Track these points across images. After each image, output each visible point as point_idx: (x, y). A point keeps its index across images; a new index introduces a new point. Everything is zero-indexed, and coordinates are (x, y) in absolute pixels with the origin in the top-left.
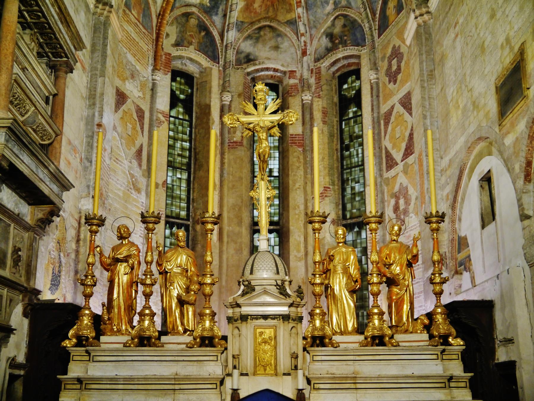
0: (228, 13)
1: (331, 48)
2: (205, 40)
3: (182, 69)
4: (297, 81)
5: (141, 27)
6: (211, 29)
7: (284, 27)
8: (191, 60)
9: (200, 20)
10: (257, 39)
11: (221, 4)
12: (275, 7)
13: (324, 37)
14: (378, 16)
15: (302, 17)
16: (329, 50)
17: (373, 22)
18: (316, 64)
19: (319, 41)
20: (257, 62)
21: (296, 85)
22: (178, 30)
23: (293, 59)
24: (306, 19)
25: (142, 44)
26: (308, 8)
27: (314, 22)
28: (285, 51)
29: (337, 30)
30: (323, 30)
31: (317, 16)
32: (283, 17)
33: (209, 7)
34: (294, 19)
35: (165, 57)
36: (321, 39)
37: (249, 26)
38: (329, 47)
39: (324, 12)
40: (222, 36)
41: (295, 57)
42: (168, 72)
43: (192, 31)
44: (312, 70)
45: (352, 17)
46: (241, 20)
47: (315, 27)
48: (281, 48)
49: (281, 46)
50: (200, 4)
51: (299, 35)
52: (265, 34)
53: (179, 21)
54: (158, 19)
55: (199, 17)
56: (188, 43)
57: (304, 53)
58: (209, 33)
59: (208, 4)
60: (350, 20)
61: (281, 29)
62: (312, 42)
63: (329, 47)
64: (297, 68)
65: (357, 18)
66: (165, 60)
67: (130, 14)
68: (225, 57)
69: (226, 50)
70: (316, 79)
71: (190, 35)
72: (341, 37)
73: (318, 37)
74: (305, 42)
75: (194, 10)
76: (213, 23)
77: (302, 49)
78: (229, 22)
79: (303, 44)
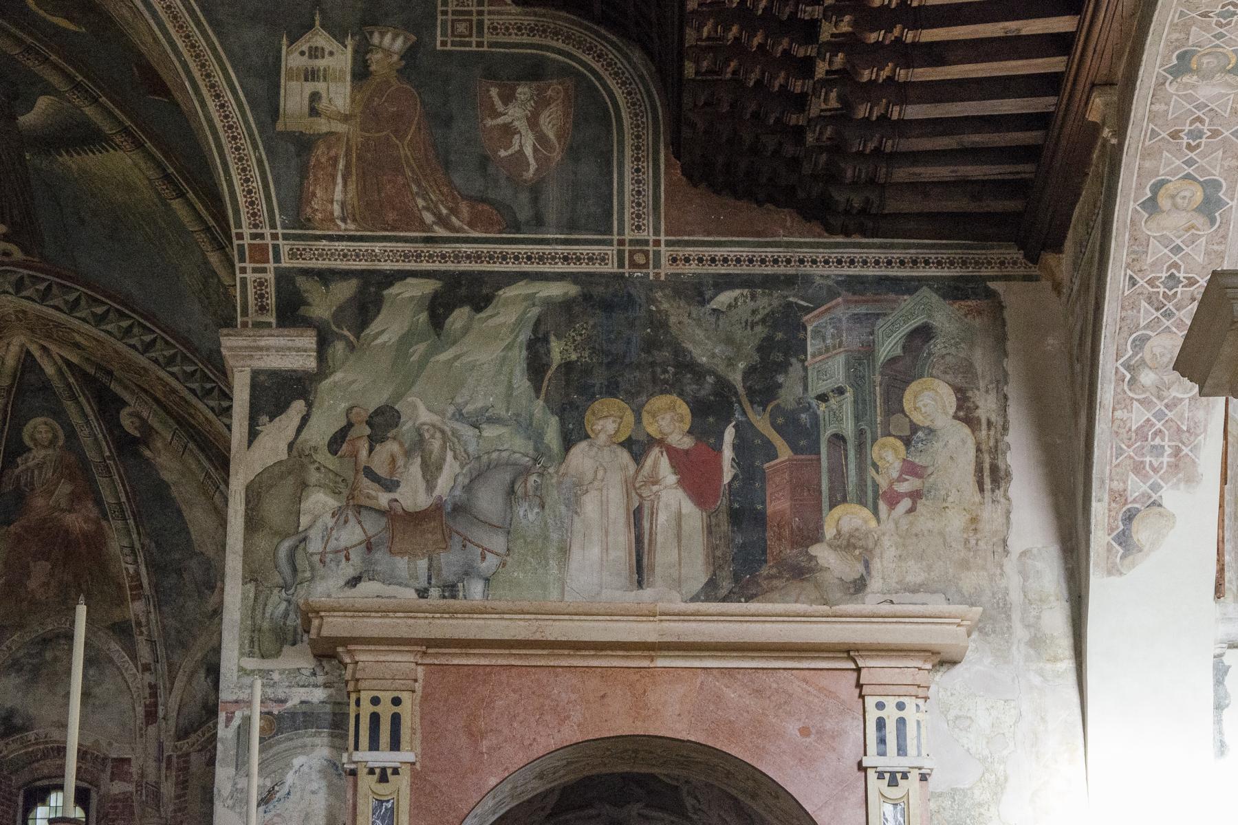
4: (131, 788)
10: (36, 672)
15: (144, 623)
19: (189, 681)
20: (31, 735)
21: (126, 799)
26: (161, 598)
27: (179, 632)
37: (15, 637)
47: (184, 645)
48: (95, 697)
57: (151, 715)
62: (173, 684)
70: (177, 784)
74: (153, 688)
77: (146, 706)
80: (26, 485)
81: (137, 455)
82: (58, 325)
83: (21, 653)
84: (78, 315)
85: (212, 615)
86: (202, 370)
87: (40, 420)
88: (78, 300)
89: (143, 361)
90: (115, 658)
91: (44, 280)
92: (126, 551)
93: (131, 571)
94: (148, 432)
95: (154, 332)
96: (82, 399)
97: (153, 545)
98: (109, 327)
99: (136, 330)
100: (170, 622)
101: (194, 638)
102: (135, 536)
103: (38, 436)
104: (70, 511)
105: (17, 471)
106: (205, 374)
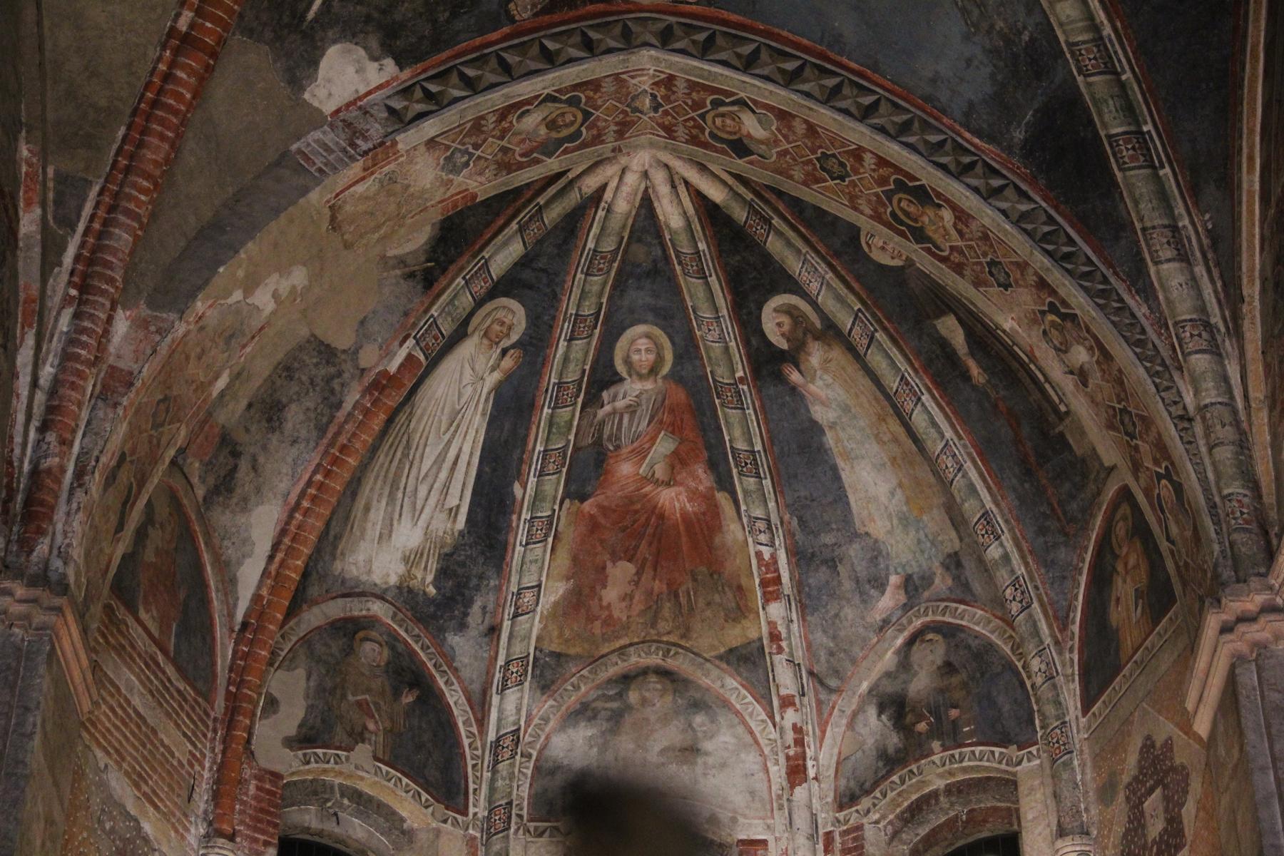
0: (507, 624)
1: (898, 751)
2: (415, 722)
3: (320, 833)
5: (170, 670)
6: (441, 682)
7: (715, 672)
8: (358, 797)
9: (400, 648)
10: (616, 718)
11: (477, 588)
12: (683, 600)
13: (872, 711)
14: (1076, 628)
15: (784, 635)
16: (891, 761)
17: (1060, 653)
18: (841, 815)
19: (851, 725)
22: (312, 684)
23: (752, 793)
24: (795, 641)
25: (170, 735)
26: (806, 603)
27: (831, 654)
28: (723, 765)
29: (921, 684)
30: (865, 686)
31: (842, 633)
32: (710, 639)
33: (432, 601)
34: (758, 644)
35: (258, 788)
36: (860, 717)
37: (584, 672)
38: (891, 750)
39: (868, 620)
40: (480, 706)
41: (761, 786)
42: (266, 844)
43: (368, 690)
44: (829, 837)
45: (977, 636)
46: (555, 647)
48: (707, 754)
49: (708, 746)
50: (399, 588)
51: (776, 703)
52: (644, 702)
53: (319, 648)
54: (236, 644)
55: (394, 637)
56: (350, 735)
57: (796, 772)
58: (430, 700)
59: (432, 590)
60: (968, 647)
61: (705, 681)
62: (824, 732)
63: (891, 750)
64: (769, 828)
65: (993, 637)
66: (255, 798)
67: (130, 620)
68: (492, 789)
69: (496, 762)
71: (359, 704)
72: (936, 712)
73: (849, 712)
74: (796, 728)
75: (377, 608)
76: (448, 658)
77: (788, 758)
78: (508, 655)
79: (790, 736)
80: (610, 439)
81: (780, 378)
82: (721, 98)
83: (593, 695)
84: (757, 71)
85: (881, 629)
86: (953, 140)
87: (641, 329)
88: (756, 53)
89: (858, 133)
90: (733, 699)
91: (702, 29)
92: (761, 525)
93: (767, 556)
94: (802, 333)
95: (874, 92)
96: (713, 280)
97: (795, 522)
98: (806, 87)
99: (846, 90)
100: (819, 637)
101: (854, 661)
102: (772, 505)
103: (635, 357)
104: (668, 485)
105: (601, 413)
106: (961, 146)
